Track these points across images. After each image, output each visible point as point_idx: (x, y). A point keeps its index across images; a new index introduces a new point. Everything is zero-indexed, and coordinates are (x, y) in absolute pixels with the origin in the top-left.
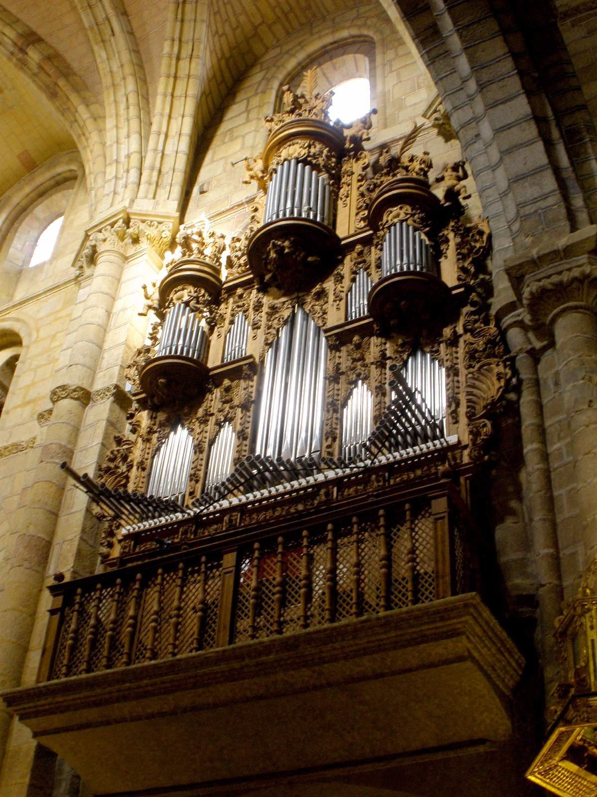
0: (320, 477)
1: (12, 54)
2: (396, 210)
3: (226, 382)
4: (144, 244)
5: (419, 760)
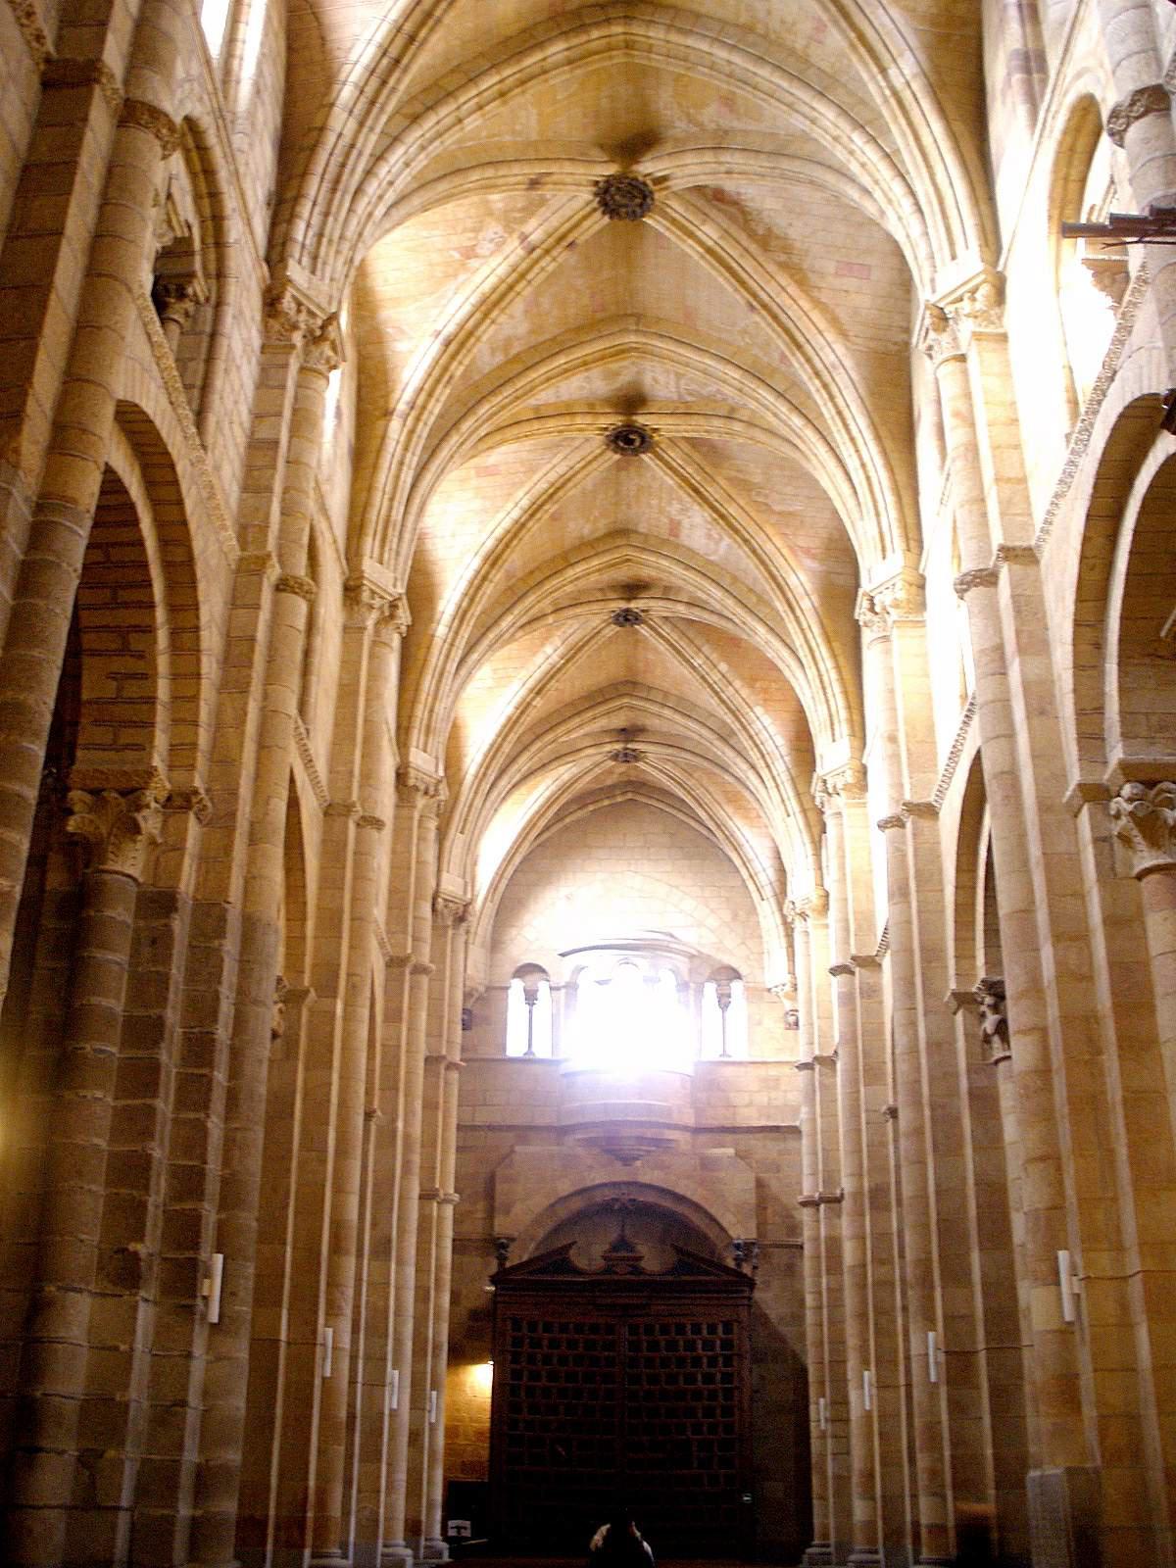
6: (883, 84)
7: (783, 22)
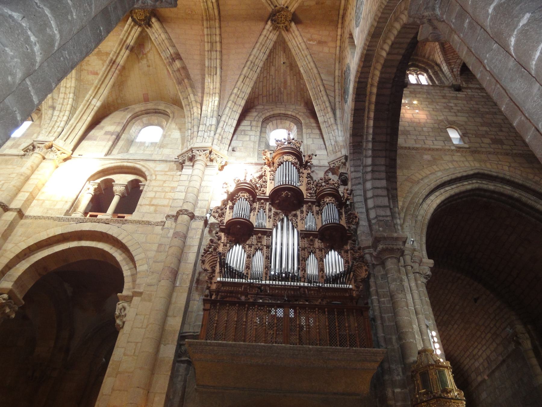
0: (302, 284)
1: (168, 58)
3: (260, 235)
4: (214, 163)
6: (91, 99)
7: (88, 61)
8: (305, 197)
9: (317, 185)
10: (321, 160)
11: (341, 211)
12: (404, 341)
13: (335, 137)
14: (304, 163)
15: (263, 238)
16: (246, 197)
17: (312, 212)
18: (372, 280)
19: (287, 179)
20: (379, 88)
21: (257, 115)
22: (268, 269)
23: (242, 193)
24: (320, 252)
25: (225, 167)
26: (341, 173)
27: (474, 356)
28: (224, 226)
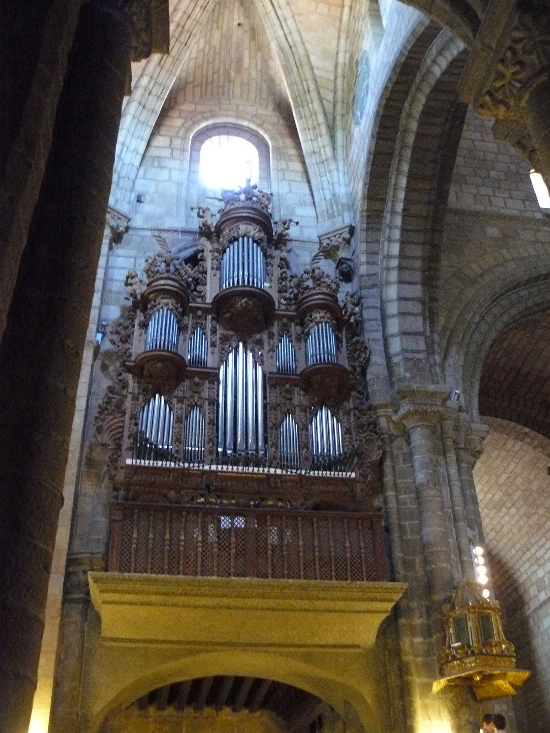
2: (322, 314)
3: (197, 379)
5: (322, 650)
8: (277, 307)
9: (298, 285)
10: (305, 227)
11: (340, 335)
12: (433, 566)
13: (333, 185)
14: (275, 238)
15: (203, 384)
16: (171, 307)
17: (290, 336)
18: (388, 463)
19: (246, 273)
20: (422, 123)
21: (183, 125)
22: (213, 444)
23: (163, 298)
24: (303, 414)
25: (125, 236)
26: (340, 260)
27: (537, 560)
28: (132, 362)
